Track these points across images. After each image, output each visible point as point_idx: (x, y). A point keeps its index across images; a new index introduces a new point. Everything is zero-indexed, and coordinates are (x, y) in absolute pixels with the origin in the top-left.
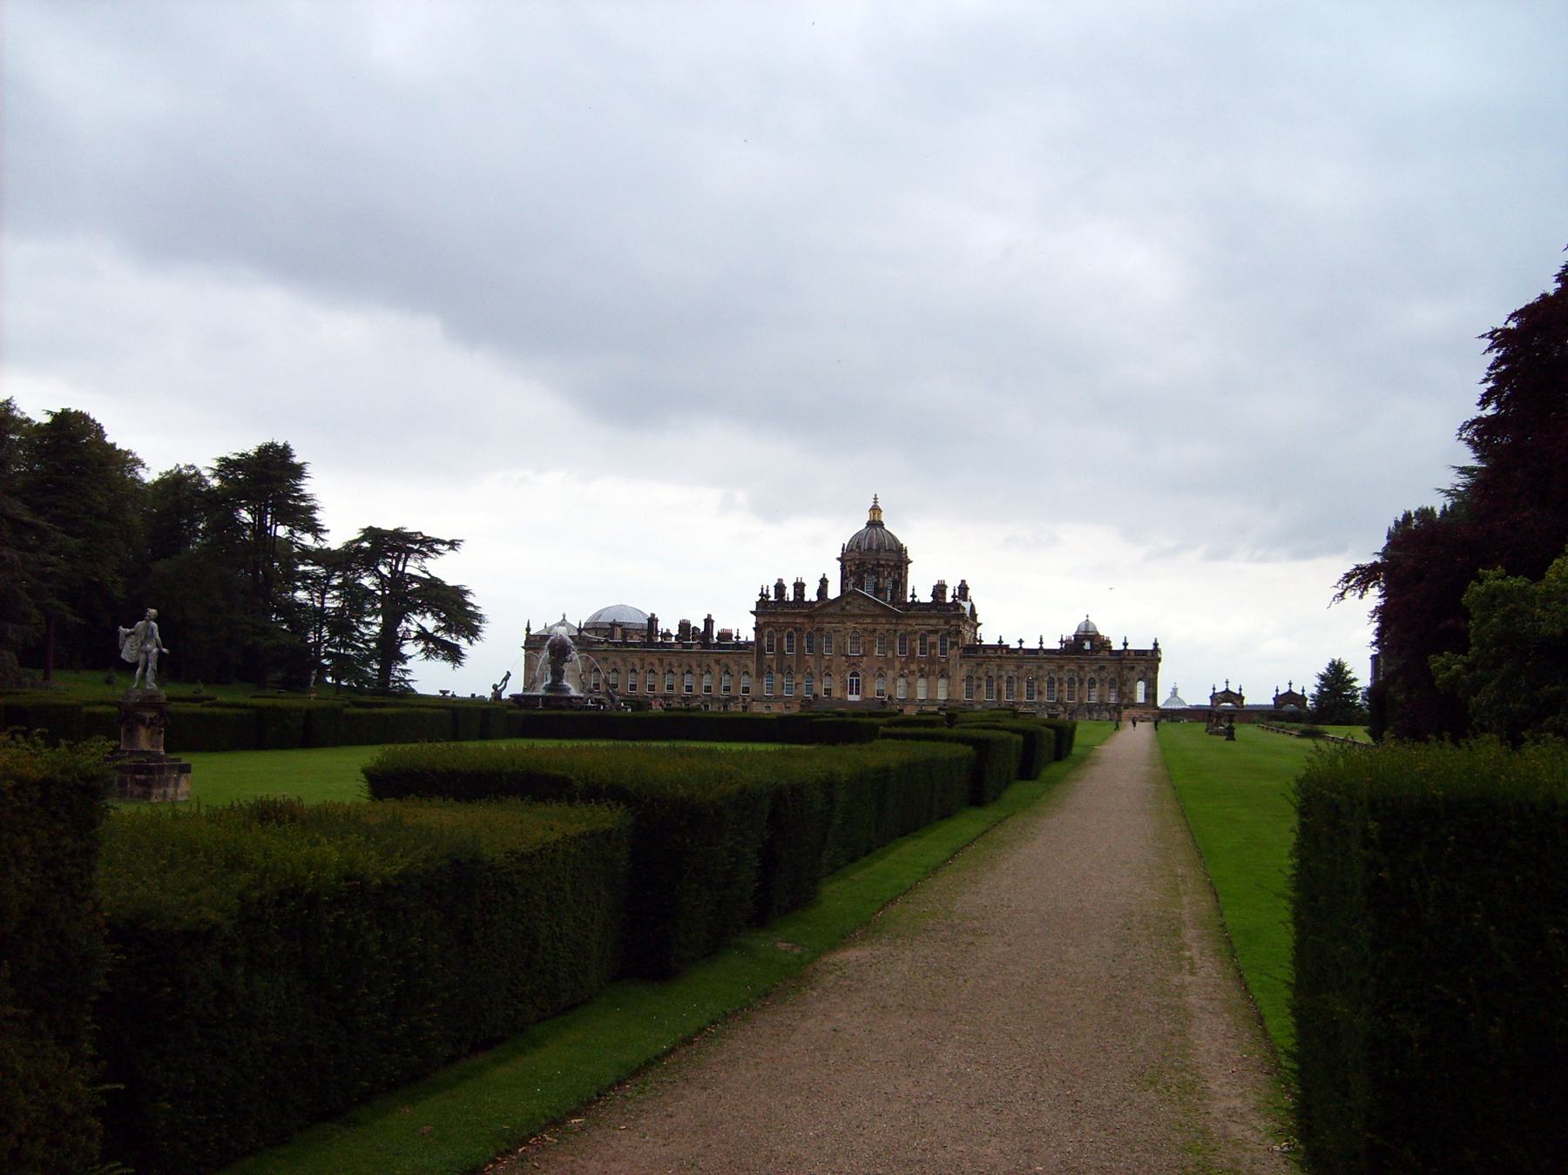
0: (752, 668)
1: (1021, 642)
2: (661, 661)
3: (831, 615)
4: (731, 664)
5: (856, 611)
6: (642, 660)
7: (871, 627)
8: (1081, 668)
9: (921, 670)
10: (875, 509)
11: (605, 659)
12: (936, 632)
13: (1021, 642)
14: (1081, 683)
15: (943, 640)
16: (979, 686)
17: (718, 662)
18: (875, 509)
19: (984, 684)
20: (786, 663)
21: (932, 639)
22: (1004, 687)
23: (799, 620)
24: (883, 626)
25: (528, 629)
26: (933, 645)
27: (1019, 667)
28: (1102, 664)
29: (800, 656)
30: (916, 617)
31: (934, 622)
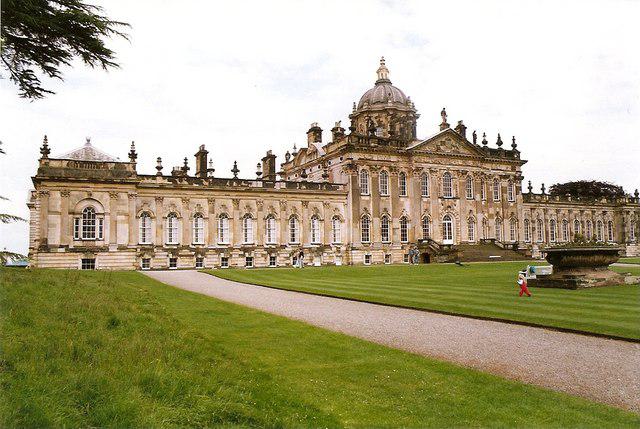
0: (345, 208)
2: (236, 202)
3: (428, 154)
4: (320, 206)
6: (211, 201)
7: (462, 169)
8: (593, 212)
10: (382, 67)
11: (159, 199)
12: (506, 177)
15: (511, 185)
16: (534, 229)
17: (305, 204)
18: (382, 67)
20: (382, 205)
21: (505, 183)
23: (394, 158)
25: (45, 151)
26: (504, 190)
27: (558, 211)
28: (605, 209)
29: (395, 201)
30: (492, 162)
31: (504, 167)
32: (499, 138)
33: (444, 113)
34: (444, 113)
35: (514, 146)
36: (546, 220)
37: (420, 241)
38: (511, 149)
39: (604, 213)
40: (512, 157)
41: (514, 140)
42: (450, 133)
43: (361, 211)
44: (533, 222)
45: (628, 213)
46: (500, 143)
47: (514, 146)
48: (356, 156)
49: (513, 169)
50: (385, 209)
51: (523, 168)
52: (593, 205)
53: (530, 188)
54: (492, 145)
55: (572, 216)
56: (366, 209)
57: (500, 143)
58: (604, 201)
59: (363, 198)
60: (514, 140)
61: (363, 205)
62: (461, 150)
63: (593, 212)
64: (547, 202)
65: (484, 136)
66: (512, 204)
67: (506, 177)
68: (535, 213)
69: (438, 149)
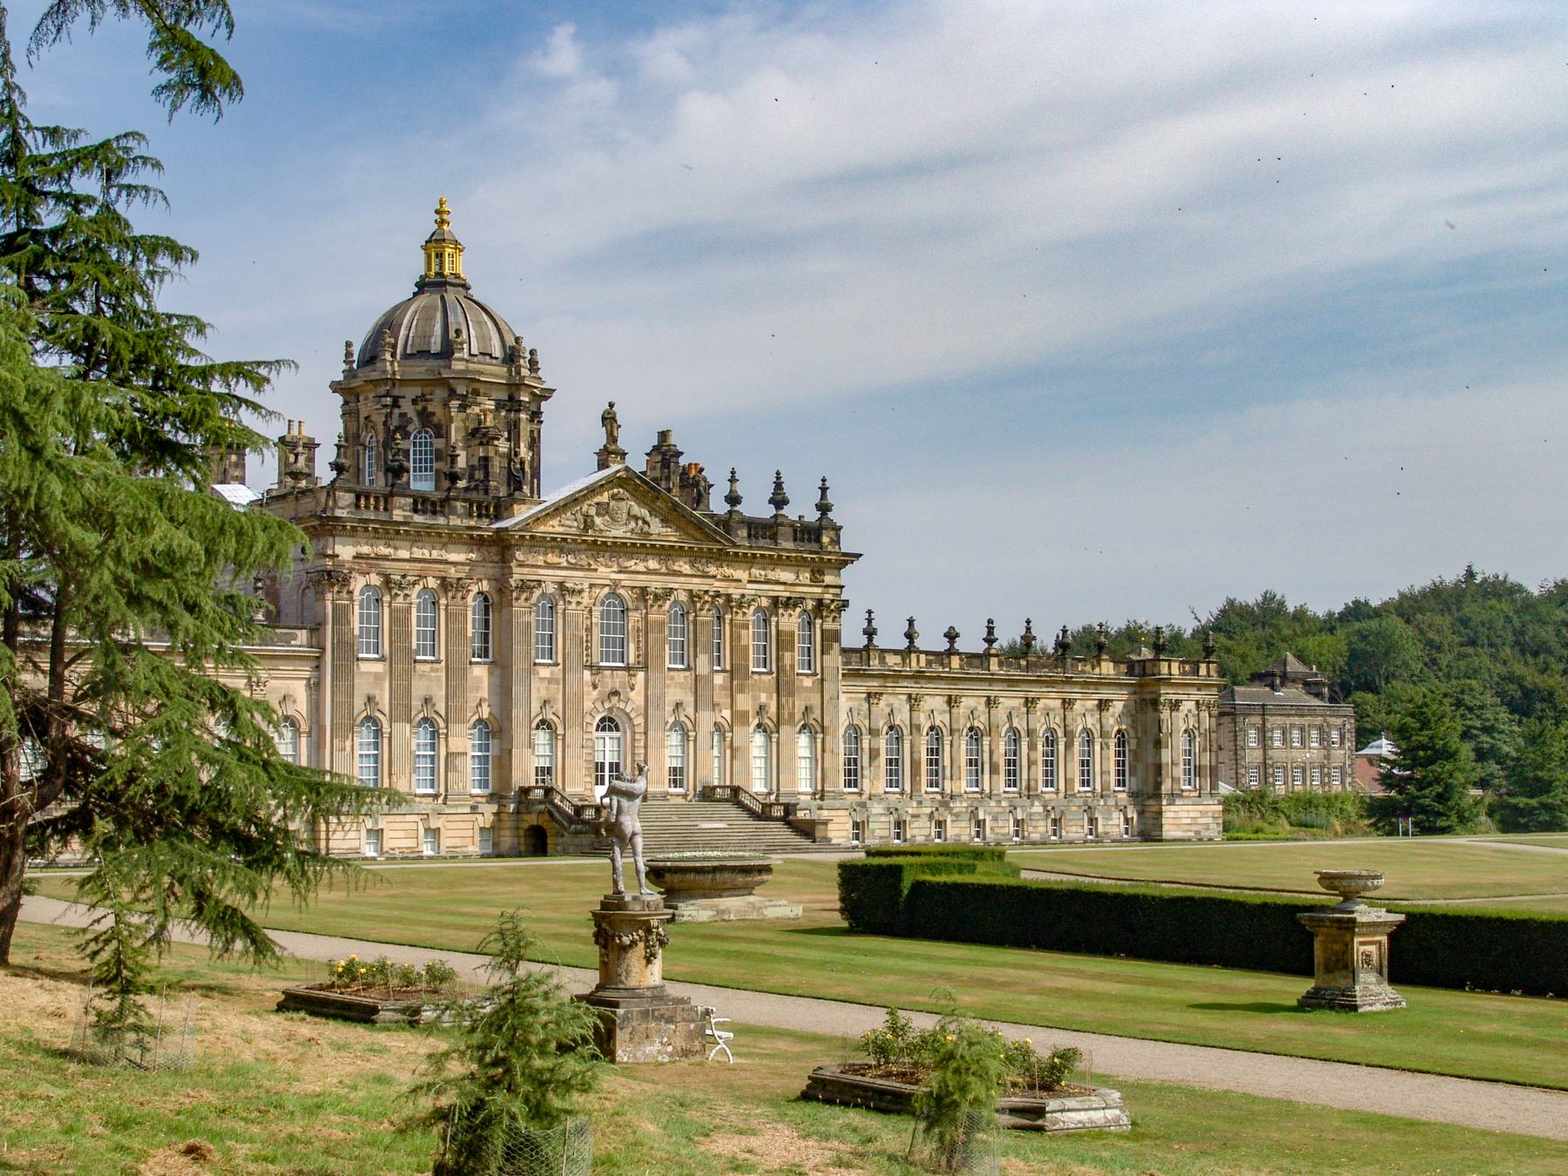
1: (951, 636)
3: (558, 544)
5: (619, 532)
8: (1067, 704)
9: (761, 709)
12: (790, 603)
13: (951, 636)
14: (1069, 746)
16: (874, 753)
19: (882, 743)
21: (790, 621)
22: (924, 757)
24: (685, 579)
26: (784, 641)
27: (951, 702)
30: (749, 561)
31: (787, 576)
32: (778, 486)
33: (609, 419)
34: (609, 419)
35: (824, 508)
36: (915, 728)
37: (525, 791)
38: (812, 516)
39: (1103, 705)
40: (815, 542)
41: (824, 490)
42: (628, 481)
43: (359, 703)
44: (873, 732)
45: (1175, 706)
46: (779, 501)
47: (824, 508)
48: (345, 551)
49: (816, 578)
50: (427, 701)
51: (847, 575)
52: (1068, 681)
53: (870, 633)
54: (756, 506)
55: (1000, 714)
56: (370, 699)
57: (779, 501)
58: (1107, 668)
59: (364, 667)
60: (824, 490)
61: (362, 688)
62: (656, 527)
63: (1067, 704)
64: (918, 676)
65: (733, 480)
66: (808, 682)
67: (790, 603)
68: (882, 706)
69: (588, 523)
